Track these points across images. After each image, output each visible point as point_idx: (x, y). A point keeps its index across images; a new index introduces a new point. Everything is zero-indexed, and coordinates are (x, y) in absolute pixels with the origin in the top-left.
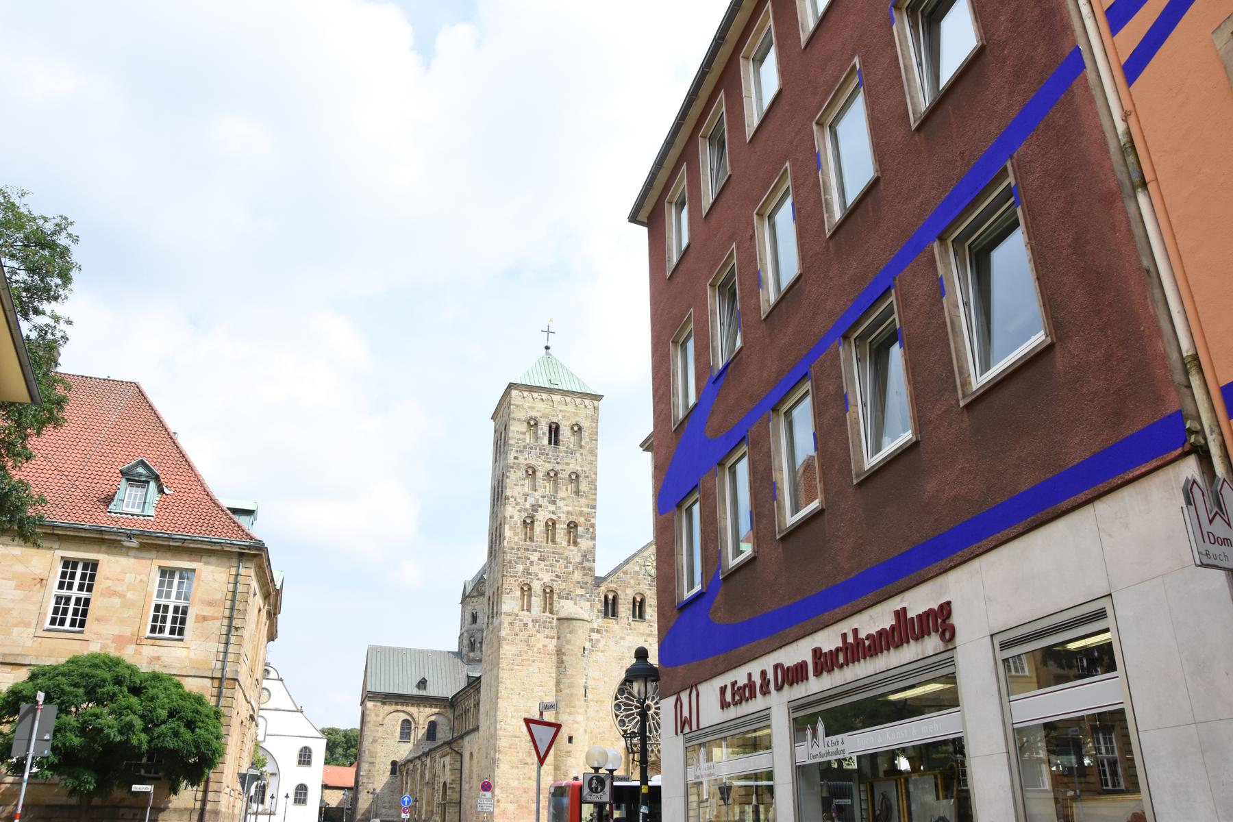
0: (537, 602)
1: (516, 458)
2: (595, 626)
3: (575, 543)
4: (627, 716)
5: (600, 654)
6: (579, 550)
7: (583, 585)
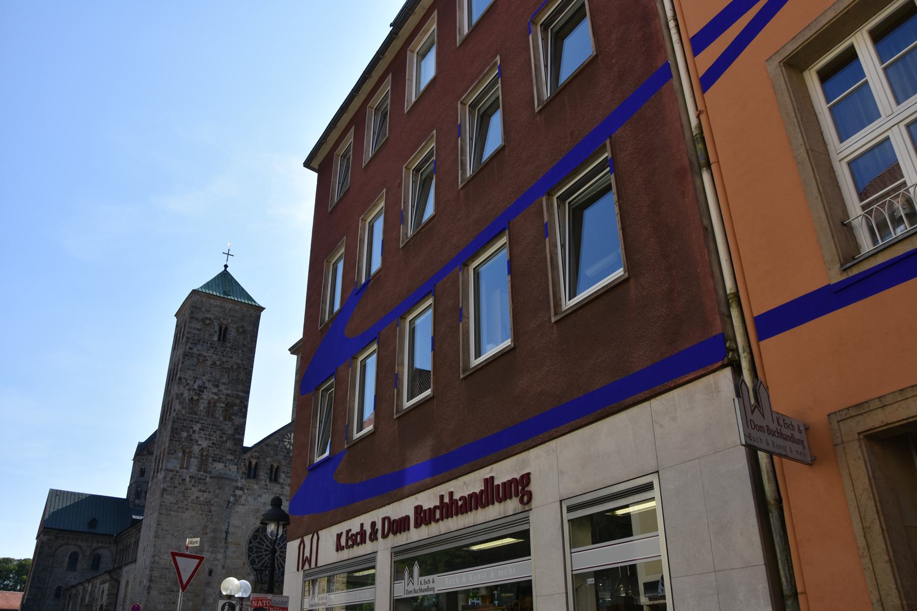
0: (194, 462)
1: (191, 348)
2: (239, 484)
3: (230, 419)
4: (257, 557)
5: (241, 507)
6: (233, 425)
7: (233, 452)
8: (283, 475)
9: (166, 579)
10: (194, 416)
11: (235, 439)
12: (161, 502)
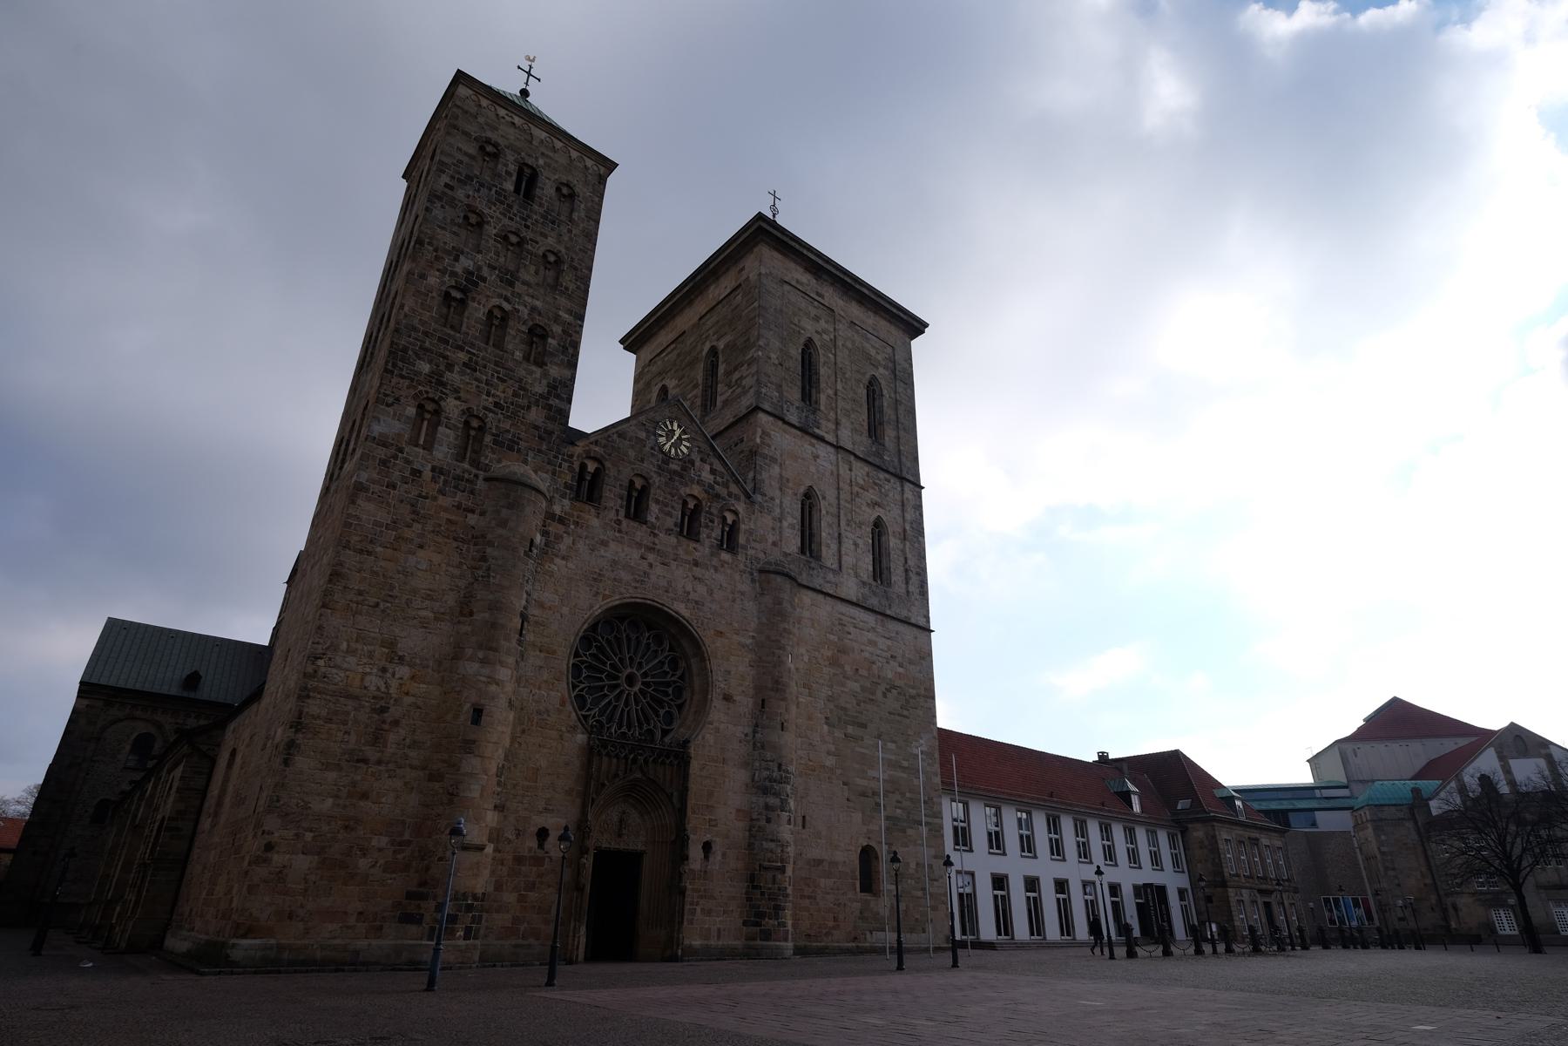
0: (447, 437)
2: (557, 509)
3: (541, 364)
5: (558, 561)
6: (545, 375)
8: (654, 508)
9: (345, 723)
10: (452, 333)
11: (550, 407)
12: (349, 516)
